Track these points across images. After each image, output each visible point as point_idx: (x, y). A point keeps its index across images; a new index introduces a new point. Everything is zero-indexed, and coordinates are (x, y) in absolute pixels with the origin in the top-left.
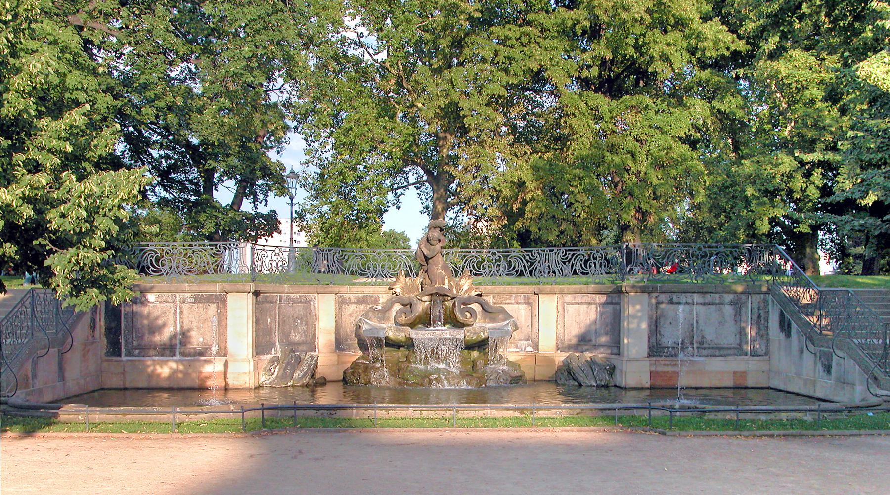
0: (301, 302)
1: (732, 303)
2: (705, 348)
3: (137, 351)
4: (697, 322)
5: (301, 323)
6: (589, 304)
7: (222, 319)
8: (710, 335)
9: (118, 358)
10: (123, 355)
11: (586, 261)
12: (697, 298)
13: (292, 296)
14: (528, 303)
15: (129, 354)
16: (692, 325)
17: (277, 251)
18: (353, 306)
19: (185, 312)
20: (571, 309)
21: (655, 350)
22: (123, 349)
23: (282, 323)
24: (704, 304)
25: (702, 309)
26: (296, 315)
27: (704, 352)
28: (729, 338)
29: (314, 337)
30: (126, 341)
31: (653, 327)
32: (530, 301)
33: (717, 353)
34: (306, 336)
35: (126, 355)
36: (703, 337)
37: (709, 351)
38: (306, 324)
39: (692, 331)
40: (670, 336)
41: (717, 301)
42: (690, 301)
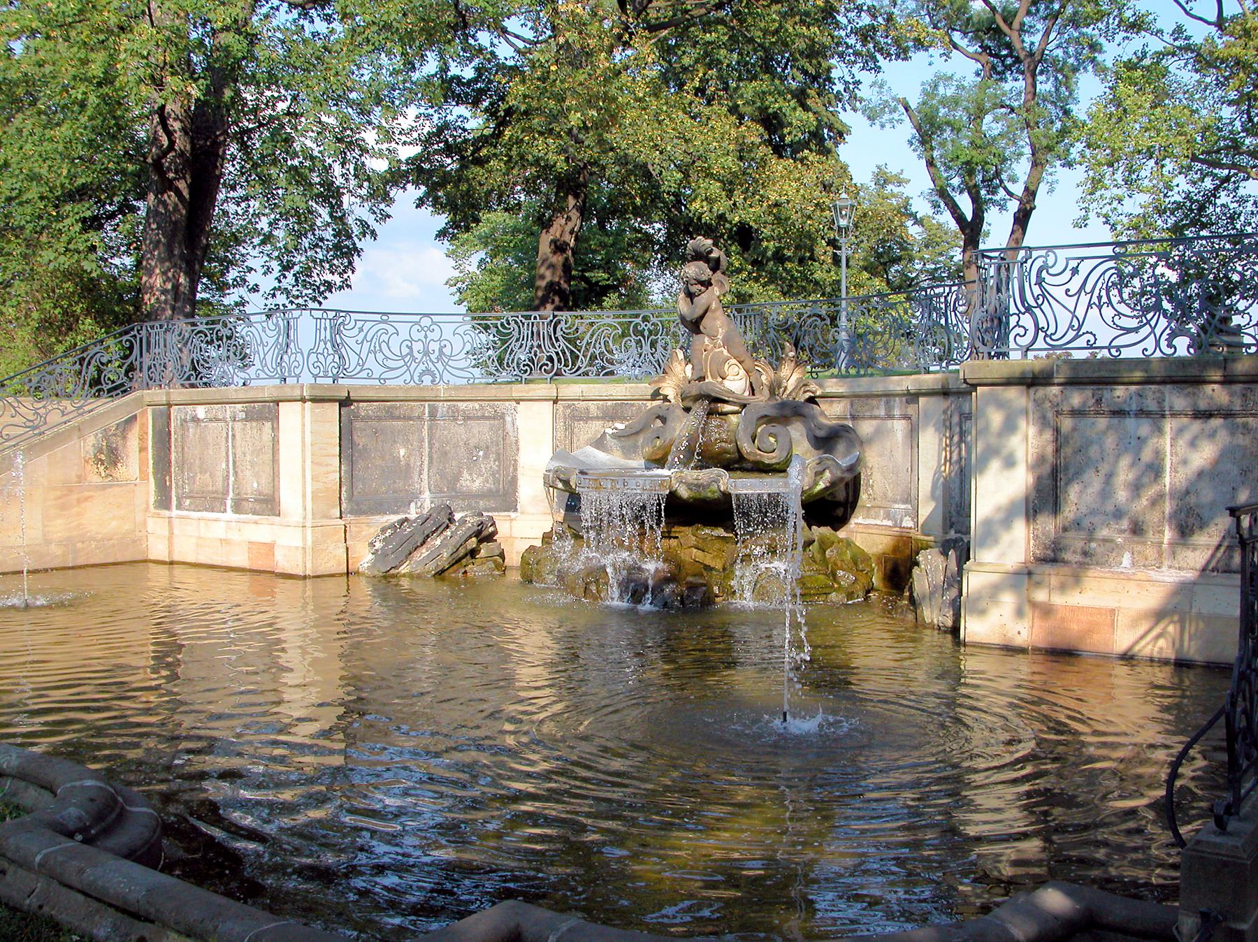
0: (483, 417)
5: (486, 456)
10: (174, 507)
15: (179, 507)
17: (426, 322)
19: (238, 437)
22: (174, 499)
26: (473, 442)
29: (513, 482)
34: (496, 481)
38: (498, 459)
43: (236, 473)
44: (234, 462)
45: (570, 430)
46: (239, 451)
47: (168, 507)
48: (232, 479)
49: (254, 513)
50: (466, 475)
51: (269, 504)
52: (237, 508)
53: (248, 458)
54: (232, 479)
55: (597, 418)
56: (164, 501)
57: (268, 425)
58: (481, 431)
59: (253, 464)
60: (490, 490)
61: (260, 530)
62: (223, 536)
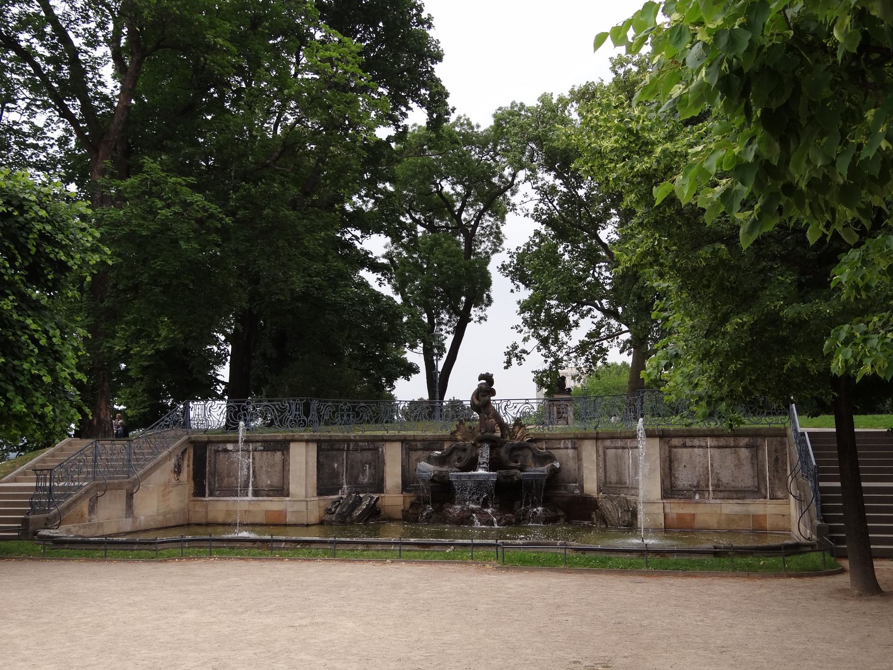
0: (370, 449)
1: (747, 446)
2: (721, 491)
3: (218, 492)
4: (712, 465)
6: (623, 448)
7: (285, 464)
8: (726, 477)
9: (202, 498)
11: (334, 413)
12: (710, 441)
13: (360, 444)
14: (574, 448)
16: (707, 468)
18: (420, 453)
19: (257, 458)
20: (611, 452)
21: (670, 491)
22: (207, 491)
23: (350, 468)
24: (719, 447)
25: (716, 452)
26: (364, 460)
27: (721, 495)
28: (746, 480)
30: (210, 484)
31: (667, 471)
32: (577, 446)
33: (735, 496)
34: (374, 479)
35: (210, 496)
36: (719, 480)
37: (726, 494)
38: (375, 468)
39: (708, 474)
40: (684, 478)
41: (732, 444)
42: (704, 444)
43: (254, 476)
44: (254, 471)
45: (408, 454)
46: (257, 466)
47: (204, 496)
48: (251, 480)
49: (268, 496)
50: (361, 476)
51: (281, 491)
52: (256, 493)
53: (264, 469)
54: (251, 480)
55: (421, 449)
56: (199, 491)
57: (279, 454)
58: (368, 455)
59: (267, 472)
60: (371, 484)
61: (274, 504)
62: (247, 508)
